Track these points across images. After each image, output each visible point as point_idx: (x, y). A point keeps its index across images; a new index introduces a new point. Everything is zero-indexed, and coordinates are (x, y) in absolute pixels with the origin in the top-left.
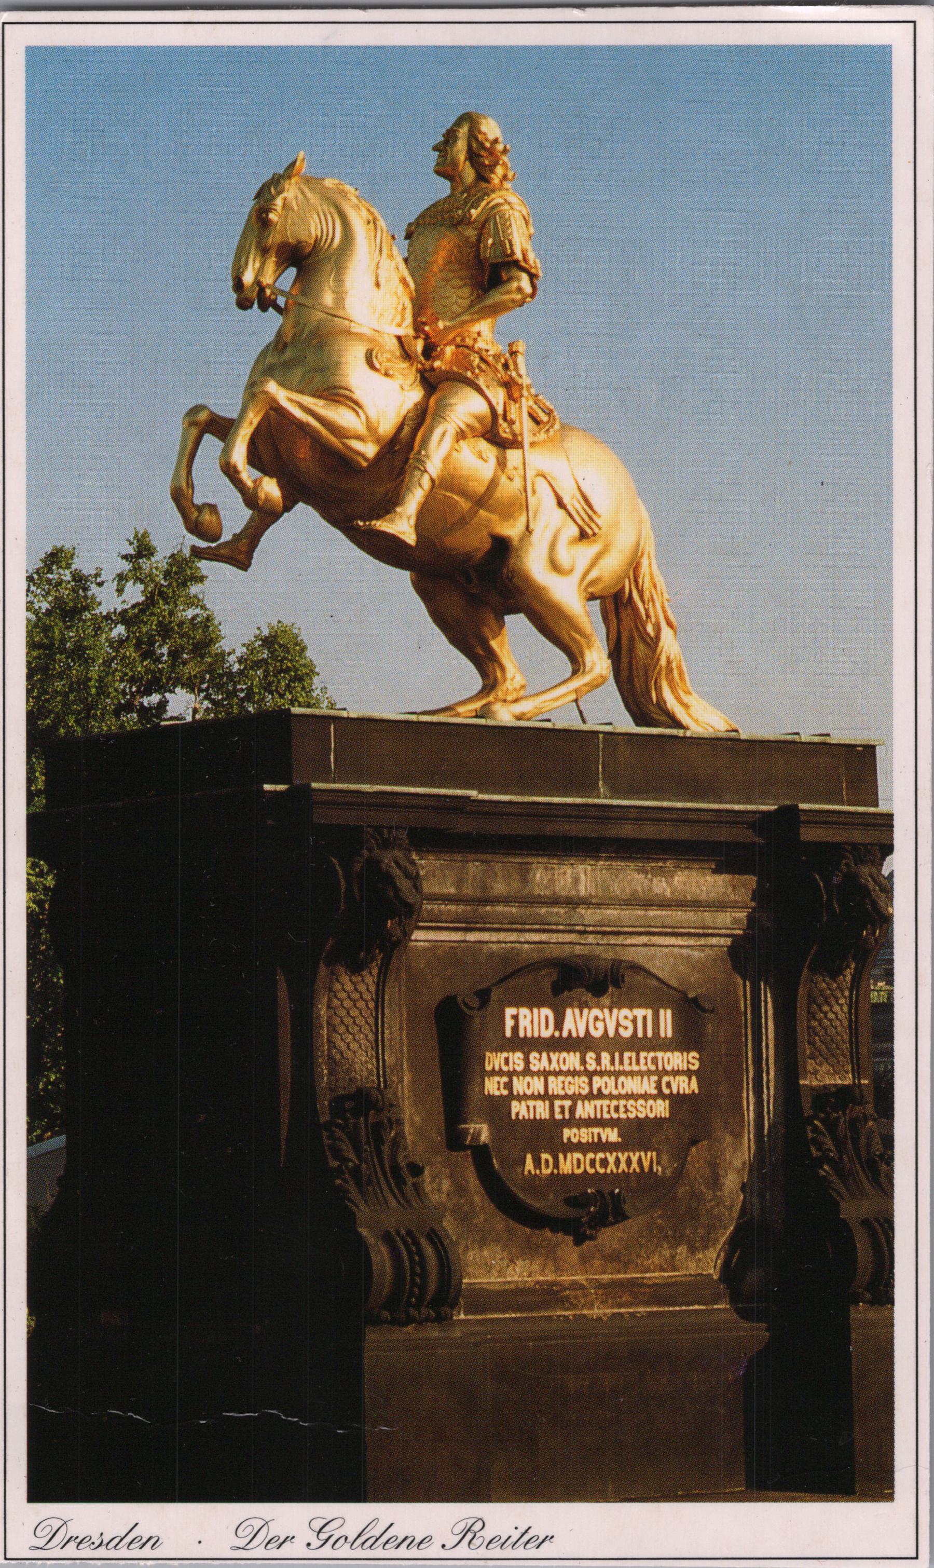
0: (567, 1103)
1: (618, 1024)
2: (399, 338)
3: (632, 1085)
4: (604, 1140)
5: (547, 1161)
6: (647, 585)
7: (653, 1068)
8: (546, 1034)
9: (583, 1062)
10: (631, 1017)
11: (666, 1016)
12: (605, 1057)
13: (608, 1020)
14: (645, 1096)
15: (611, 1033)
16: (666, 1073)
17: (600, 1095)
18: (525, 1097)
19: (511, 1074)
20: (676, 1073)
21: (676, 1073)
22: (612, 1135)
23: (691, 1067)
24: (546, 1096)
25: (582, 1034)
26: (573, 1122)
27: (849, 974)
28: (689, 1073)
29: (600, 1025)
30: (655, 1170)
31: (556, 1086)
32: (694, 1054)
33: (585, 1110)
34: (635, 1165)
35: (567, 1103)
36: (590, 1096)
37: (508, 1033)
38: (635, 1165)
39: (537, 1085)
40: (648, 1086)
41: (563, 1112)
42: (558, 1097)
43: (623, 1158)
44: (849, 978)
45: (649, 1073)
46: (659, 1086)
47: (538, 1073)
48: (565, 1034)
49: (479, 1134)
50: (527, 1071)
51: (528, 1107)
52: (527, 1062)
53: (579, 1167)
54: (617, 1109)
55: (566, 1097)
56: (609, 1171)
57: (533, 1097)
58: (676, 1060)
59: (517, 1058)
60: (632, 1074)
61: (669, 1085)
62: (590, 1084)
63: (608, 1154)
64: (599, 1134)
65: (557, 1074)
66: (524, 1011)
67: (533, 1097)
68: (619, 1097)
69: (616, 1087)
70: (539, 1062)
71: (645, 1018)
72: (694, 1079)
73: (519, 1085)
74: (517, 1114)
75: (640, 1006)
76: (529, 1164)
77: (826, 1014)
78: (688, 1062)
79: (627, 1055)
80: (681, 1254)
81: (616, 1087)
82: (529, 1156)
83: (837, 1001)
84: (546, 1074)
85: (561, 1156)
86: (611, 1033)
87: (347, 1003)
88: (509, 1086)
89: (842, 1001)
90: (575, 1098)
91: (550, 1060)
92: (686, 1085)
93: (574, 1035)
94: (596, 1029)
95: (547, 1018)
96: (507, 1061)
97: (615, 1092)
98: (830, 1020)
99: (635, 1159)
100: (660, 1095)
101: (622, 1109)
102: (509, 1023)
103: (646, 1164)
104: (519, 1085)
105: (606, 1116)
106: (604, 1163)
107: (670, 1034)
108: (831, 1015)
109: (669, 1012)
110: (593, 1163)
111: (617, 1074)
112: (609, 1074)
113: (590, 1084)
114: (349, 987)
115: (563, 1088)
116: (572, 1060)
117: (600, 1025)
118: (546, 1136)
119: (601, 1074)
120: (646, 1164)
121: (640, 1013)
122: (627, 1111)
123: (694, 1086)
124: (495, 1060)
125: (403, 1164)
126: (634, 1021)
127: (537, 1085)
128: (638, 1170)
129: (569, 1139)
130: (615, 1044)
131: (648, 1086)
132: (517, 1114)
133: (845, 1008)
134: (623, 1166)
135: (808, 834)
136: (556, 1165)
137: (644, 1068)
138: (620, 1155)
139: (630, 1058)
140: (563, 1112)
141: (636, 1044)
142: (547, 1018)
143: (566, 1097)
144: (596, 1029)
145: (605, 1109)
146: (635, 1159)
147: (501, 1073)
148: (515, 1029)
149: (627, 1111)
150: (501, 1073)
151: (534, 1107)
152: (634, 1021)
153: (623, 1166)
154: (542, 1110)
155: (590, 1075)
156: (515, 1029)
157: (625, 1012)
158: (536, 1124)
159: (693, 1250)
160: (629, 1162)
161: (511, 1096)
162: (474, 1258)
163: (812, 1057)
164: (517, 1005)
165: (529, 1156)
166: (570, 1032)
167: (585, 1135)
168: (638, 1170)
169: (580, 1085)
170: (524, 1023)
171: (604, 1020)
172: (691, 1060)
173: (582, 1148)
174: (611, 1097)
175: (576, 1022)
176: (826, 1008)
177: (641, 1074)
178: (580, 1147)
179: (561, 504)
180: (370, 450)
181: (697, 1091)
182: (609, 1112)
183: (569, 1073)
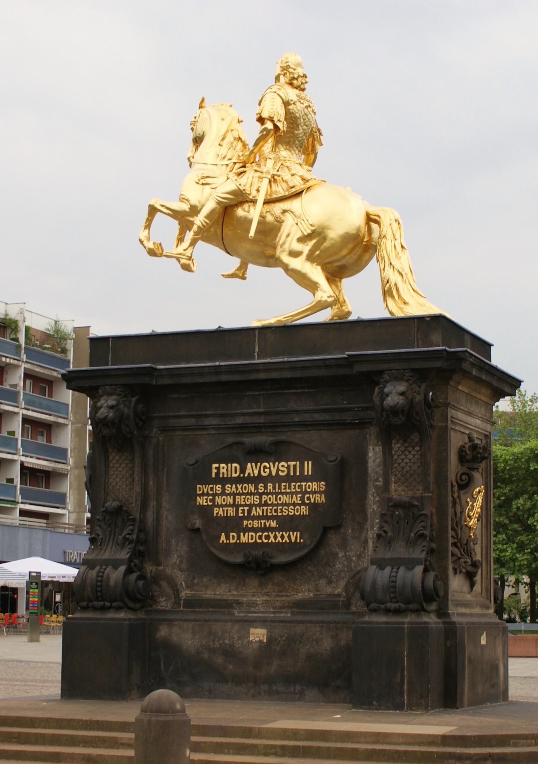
0: (246, 508)
1: (278, 470)
3: (285, 499)
4: (268, 525)
5: (233, 536)
8: (234, 475)
9: (256, 488)
10: (286, 465)
12: (270, 486)
13: (272, 468)
14: (294, 505)
15: (274, 474)
16: (309, 493)
17: (266, 504)
18: (222, 506)
19: (214, 495)
22: (273, 524)
25: (256, 475)
26: (249, 517)
28: (320, 492)
29: (267, 470)
30: (298, 541)
32: (323, 483)
33: (257, 512)
34: (286, 539)
35: (246, 508)
36: (260, 505)
37: (214, 476)
40: (297, 499)
42: (241, 506)
43: (279, 535)
45: (297, 493)
46: (302, 499)
47: (230, 494)
48: (246, 475)
49: (195, 524)
50: (223, 493)
51: (223, 511)
52: (223, 489)
53: (252, 539)
54: (276, 511)
55: (246, 505)
56: (270, 541)
57: (226, 506)
58: (314, 486)
59: (218, 488)
60: (286, 493)
61: (309, 498)
62: (261, 499)
63: (270, 533)
64: (265, 523)
65: (240, 494)
66: (222, 465)
67: (226, 506)
68: (278, 505)
69: (276, 500)
71: (295, 466)
72: (323, 495)
73: (218, 500)
76: (223, 538)
78: (320, 487)
79: (283, 484)
80: (322, 584)
81: (276, 500)
82: (223, 534)
83: (410, 452)
84: (234, 495)
85: (242, 534)
86: (274, 474)
88: (213, 500)
90: (250, 506)
91: (237, 488)
93: (252, 475)
94: (265, 472)
95: (236, 467)
97: (275, 502)
99: (286, 535)
100: (303, 503)
102: (214, 471)
103: (293, 540)
105: (269, 514)
106: (268, 537)
107: (310, 473)
109: (310, 462)
111: (277, 494)
112: (272, 494)
113: (261, 499)
115: (244, 501)
116: (251, 488)
117: (267, 470)
118: (234, 524)
119: (267, 494)
120: (293, 540)
121: (292, 463)
122: (282, 511)
123: (323, 499)
124: (201, 488)
126: (288, 467)
127: (230, 500)
128: (288, 541)
130: (276, 479)
131: (297, 499)
132: (217, 514)
134: (279, 539)
136: (239, 538)
137: (293, 490)
138: (284, 533)
141: (289, 479)
142: (236, 467)
143: (246, 505)
145: (269, 511)
146: (286, 535)
148: (218, 474)
150: (208, 494)
151: (227, 510)
152: (288, 467)
153: (279, 539)
154: (231, 512)
155: (261, 495)
156: (218, 474)
158: (227, 519)
159: (330, 582)
160: (282, 537)
161: (214, 505)
162: (198, 582)
165: (223, 534)
166: (249, 474)
167: (256, 524)
168: (288, 541)
169: (256, 500)
170: (222, 471)
171: (270, 468)
172: (321, 486)
174: (272, 505)
175: (252, 470)
177: (292, 493)
181: (324, 501)
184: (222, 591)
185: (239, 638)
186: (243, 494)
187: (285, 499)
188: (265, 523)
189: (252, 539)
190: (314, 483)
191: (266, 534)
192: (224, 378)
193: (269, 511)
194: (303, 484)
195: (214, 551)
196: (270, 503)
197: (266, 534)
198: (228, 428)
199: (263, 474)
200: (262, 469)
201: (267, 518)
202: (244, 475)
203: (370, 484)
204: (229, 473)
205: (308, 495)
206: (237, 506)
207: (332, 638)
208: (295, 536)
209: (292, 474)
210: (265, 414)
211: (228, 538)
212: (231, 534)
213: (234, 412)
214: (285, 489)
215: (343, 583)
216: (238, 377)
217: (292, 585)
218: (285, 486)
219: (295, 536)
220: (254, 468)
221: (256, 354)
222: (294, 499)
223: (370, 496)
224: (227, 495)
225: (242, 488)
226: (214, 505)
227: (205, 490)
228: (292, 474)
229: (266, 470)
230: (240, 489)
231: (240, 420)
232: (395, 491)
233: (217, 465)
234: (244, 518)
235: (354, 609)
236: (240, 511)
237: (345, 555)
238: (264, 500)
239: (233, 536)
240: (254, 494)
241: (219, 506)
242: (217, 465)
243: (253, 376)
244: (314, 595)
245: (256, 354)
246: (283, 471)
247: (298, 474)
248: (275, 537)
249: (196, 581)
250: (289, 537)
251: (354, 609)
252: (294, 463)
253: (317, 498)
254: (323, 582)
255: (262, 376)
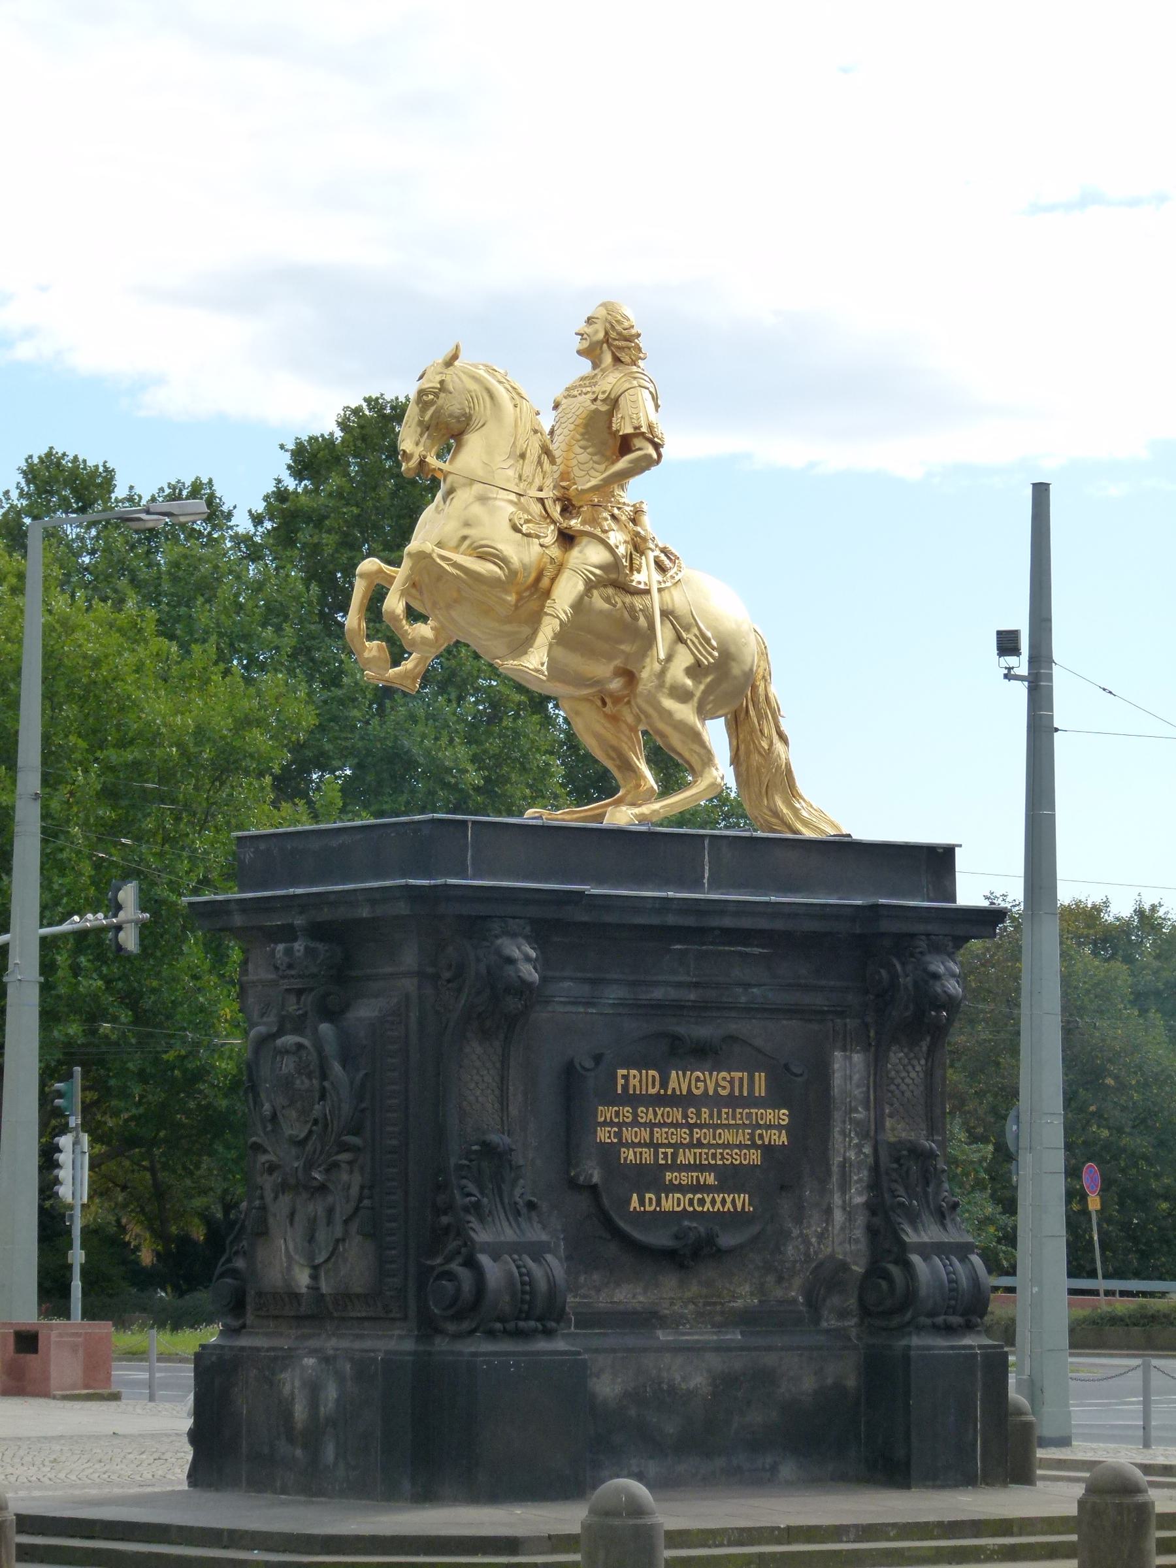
1: (717, 1084)
2: (541, 501)
3: (727, 1136)
5: (650, 1199)
6: (763, 705)
7: (747, 1122)
8: (652, 1091)
9: (685, 1116)
11: (760, 1079)
14: (740, 1146)
15: (711, 1093)
18: (634, 1145)
19: (620, 1125)
20: (769, 1127)
21: (769, 1127)
22: (711, 1179)
23: (782, 1123)
24: (654, 1145)
25: (684, 1093)
27: (924, 1046)
28: (779, 1127)
31: (659, 1135)
34: (729, 1205)
35: (670, 1151)
36: (691, 1146)
37: (619, 1091)
38: (729, 1205)
39: (645, 1134)
41: (666, 1158)
44: (925, 1049)
46: (752, 1135)
47: (645, 1125)
48: (669, 1092)
49: (591, 1176)
50: (635, 1123)
51: (635, 1153)
52: (635, 1115)
53: (679, 1205)
54: (714, 1156)
55: (669, 1145)
57: (639, 1145)
58: (770, 1115)
60: (728, 1126)
61: (761, 1137)
62: (691, 1135)
64: (697, 1177)
66: (633, 1072)
67: (639, 1145)
68: (718, 1146)
69: (714, 1139)
70: (646, 1114)
71: (741, 1079)
73: (628, 1134)
74: (626, 1159)
75: (737, 1070)
77: (903, 1079)
79: (725, 1110)
81: (714, 1139)
82: (635, 1195)
83: (914, 1067)
84: (652, 1125)
86: (711, 1093)
87: (478, 1064)
88: (619, 1135)
89: (918, 1068)
91: (655, 1114)
92: (776, 1137)
94: (697, 1088)
96: (617, 1114)
98: (908, 1085)
99: (729, 1200)
100: (754, 1145)
101: (719, 1157)
102: (621, 1082)
104: (628, 1134)
106: (702, 1202)
108: (908, 1081)
109: (763, 1074)
110: (691, 1202)
111: (716, 1127)
113: (691, 1135)
114: (479, 1050)
116: (677, 1115)
118: (650, 1178)
119: (701, 1126)
122: (723, 1158)
123: (784, 1139)
124: (606, 1113)
125: (520, 1201)
126: (731, 1082)
127: (645, 1134)
129: (671, 1181)
130: (715, 1101)
131: (743, 1137)
133: (922, 1075)
134: (718, 1205)
135: (885, 926)
136: (659, 1203)
139: (727, 1113)
140: (666, 1158)
141: (733, 1101)
143: (669, 1145)
144: (697, 1088)
146: (729, 1200)
147: (611, 1124)
148: (625, 1087)
149: (723, 1158)
150: (611, 1124)
151: (641, 1153)
152: (731, 1082)
153: (718, 1205)
154: (647, 1156)
156: (625, 1087)
157: (724, 1074)
158: (640, 1168)
159: (780, 1280)
160: (724, 1202)
161: (621, 1144)
163: (891, 1116)
164: (628, 1066)
165: (635, 1195)
167: (685, 1178)
170: (633, 1082)
171: (705, 1081)
173: (680, 1188)
174: (710, 1146)
175: (678, 1082)
176: (904, 1074)
177: (736, 1126)
178: (680, 1188)
179: (680, 639)
180: (511, 598)
182: (707, 1159)
183: (671, 1125)
184: (628, 1295)
185: (684, 1379)
186: (665, 1125)
187: (727, 1136)
188: (697, 1177)
189: (679, 1205)
190: (769, 1111)
191: (700, 1196)
192: (671, 920)
193: (703, 1155)
194: (754, 1111)
195: (622, 1224)
196: (705, 1142)
197: (700, 1196)
198: (640, 1006)
199: (695, 1092)
200: (693, 1082)
201: (701, 1168)
202: (666, 1091)
203: (837, 1115)
204: (644, 1088)
205: (759, 1131)
206: (656, 1147)
207: (816, 1374)
208: (742, 1201)
209: (737, 1094)
210: (696, 985)
211: (642, 1202)
212: (648, 1196)
213: (655, 978)
214: (727, 1119)
215: (797, 1282)
216: (690, 921)
217: (728, 1285)
218: (727, 1113)
219: (742, 1201)
220: (681, 1079)
221: (705, 881)
222: (740, 1138)
223: (836, 1135)
224: (640, 1125)
225: (662, 1115)
226: (621, 1144)
227: (608, 1116)
228: (737, 1094)
229: (700, 1084)
230: (659, 1116)
231: (658, 994)
232: (893, 1129)
233: (625, 1072)
234: (667, 1167)
235: (824, 1324)
236: (661, 1156)
237: (801, 1233)
238: (696, 1136)
239: (650, 1199)
240: (681, 1126)
241: (628, 1145)
242: (625, 1072)
243: (715, 922)
244: (760, 1301)
245: (705, 881)
246: (724, 1088)
247: (745, 1094)
248: (713, 1202)
249: (582, 1279)
250: (733, 1202)
251: (824, 1324)
252: (740, 1074)
253: (773, 1137)
254: (770, 1279)
255: (728, 922)
